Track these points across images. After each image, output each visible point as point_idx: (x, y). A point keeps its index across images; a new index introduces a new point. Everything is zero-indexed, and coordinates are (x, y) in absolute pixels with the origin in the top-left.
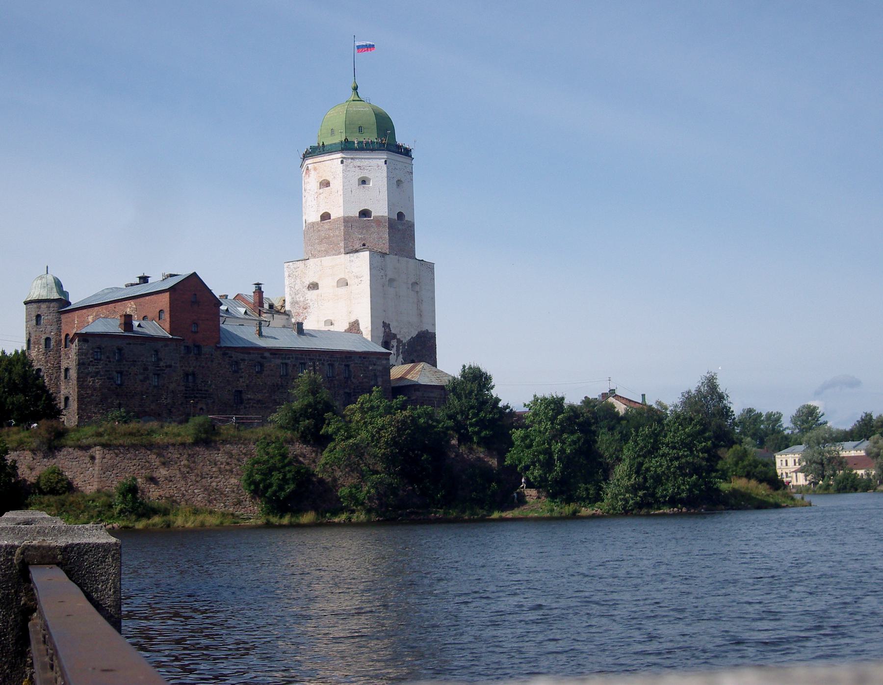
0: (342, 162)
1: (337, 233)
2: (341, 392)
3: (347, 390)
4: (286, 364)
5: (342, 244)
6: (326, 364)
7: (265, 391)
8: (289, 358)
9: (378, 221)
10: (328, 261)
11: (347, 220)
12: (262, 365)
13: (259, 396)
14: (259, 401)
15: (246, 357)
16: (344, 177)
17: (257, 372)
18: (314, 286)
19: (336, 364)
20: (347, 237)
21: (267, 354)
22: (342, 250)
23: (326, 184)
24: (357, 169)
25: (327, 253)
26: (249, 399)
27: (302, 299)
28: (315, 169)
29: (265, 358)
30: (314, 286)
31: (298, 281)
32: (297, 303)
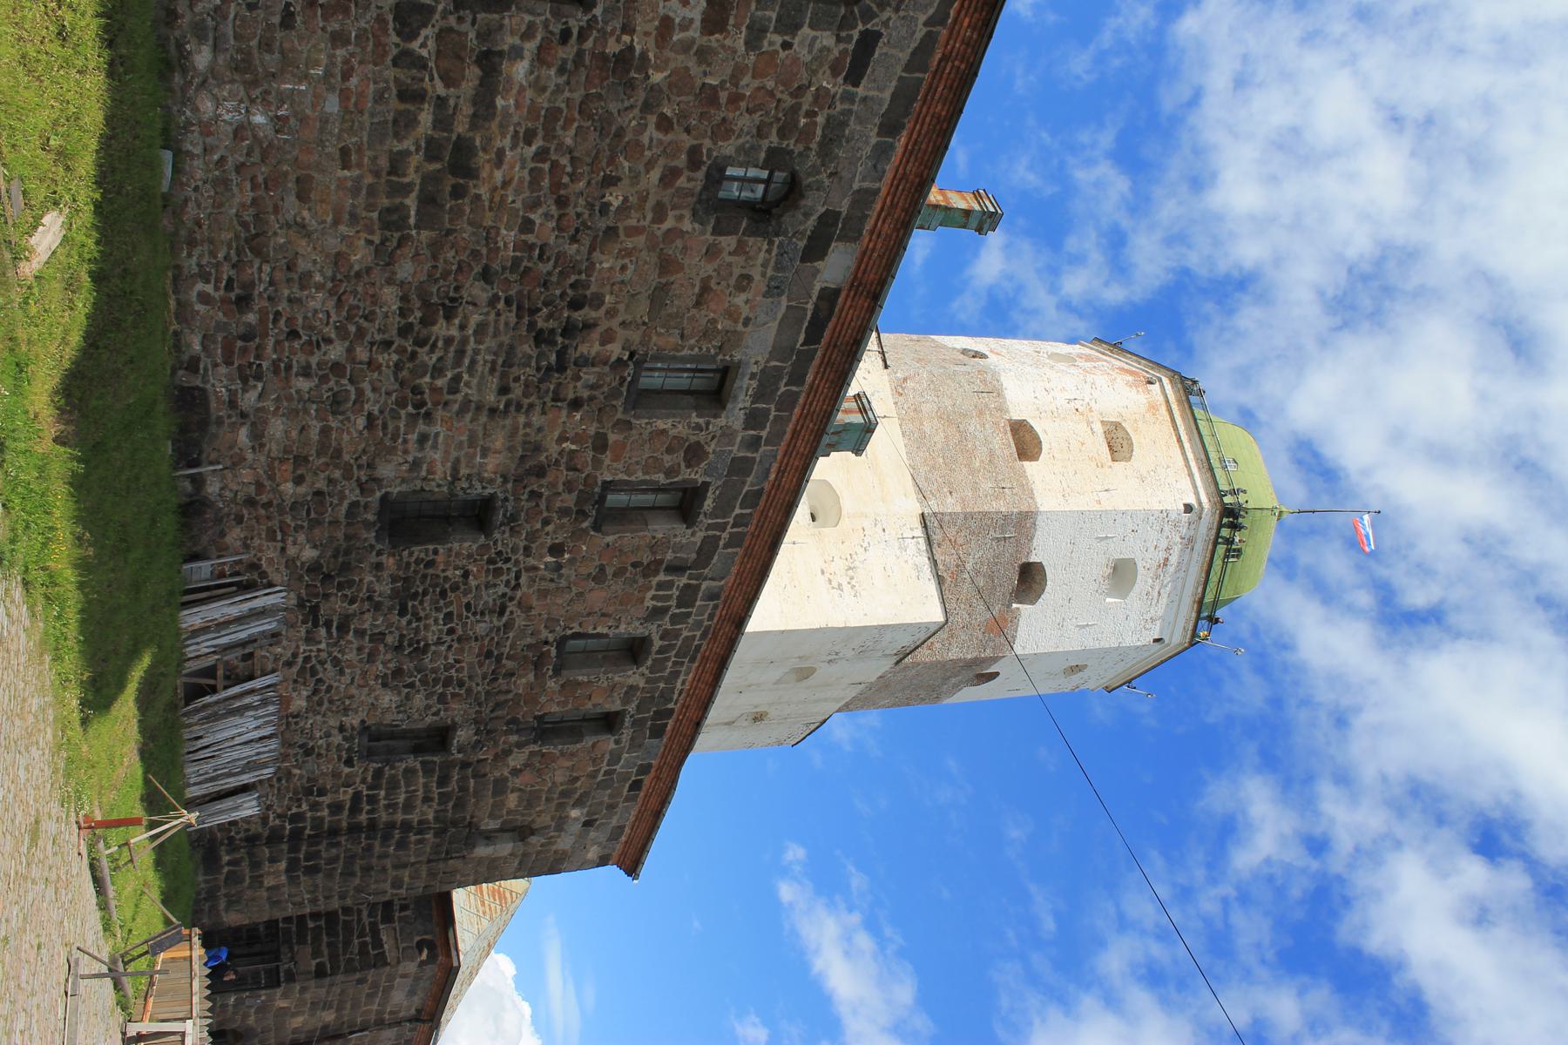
0: (1188, 508)
2: (457, 710)
3: (463, 735)
4: (715, 394)
5: (951, 505)
6: (653, 630)
7: (545, 230)
8: (754, 419)
9: (1001, 628)
11: (1023, 523)
12: (763, 215)
13: (506, 168)
14: (460, 161)
15: (879, 88)
16: (1147, 515)
17: (717, 176)
19: (635, 677)
20: (976, 523)
21: (836, 266)
22: (934, 505)
23: (1118, 443)
24: (1162, 555)
26: (490, 61)
28: (1153, 408)
29: (816, 249)
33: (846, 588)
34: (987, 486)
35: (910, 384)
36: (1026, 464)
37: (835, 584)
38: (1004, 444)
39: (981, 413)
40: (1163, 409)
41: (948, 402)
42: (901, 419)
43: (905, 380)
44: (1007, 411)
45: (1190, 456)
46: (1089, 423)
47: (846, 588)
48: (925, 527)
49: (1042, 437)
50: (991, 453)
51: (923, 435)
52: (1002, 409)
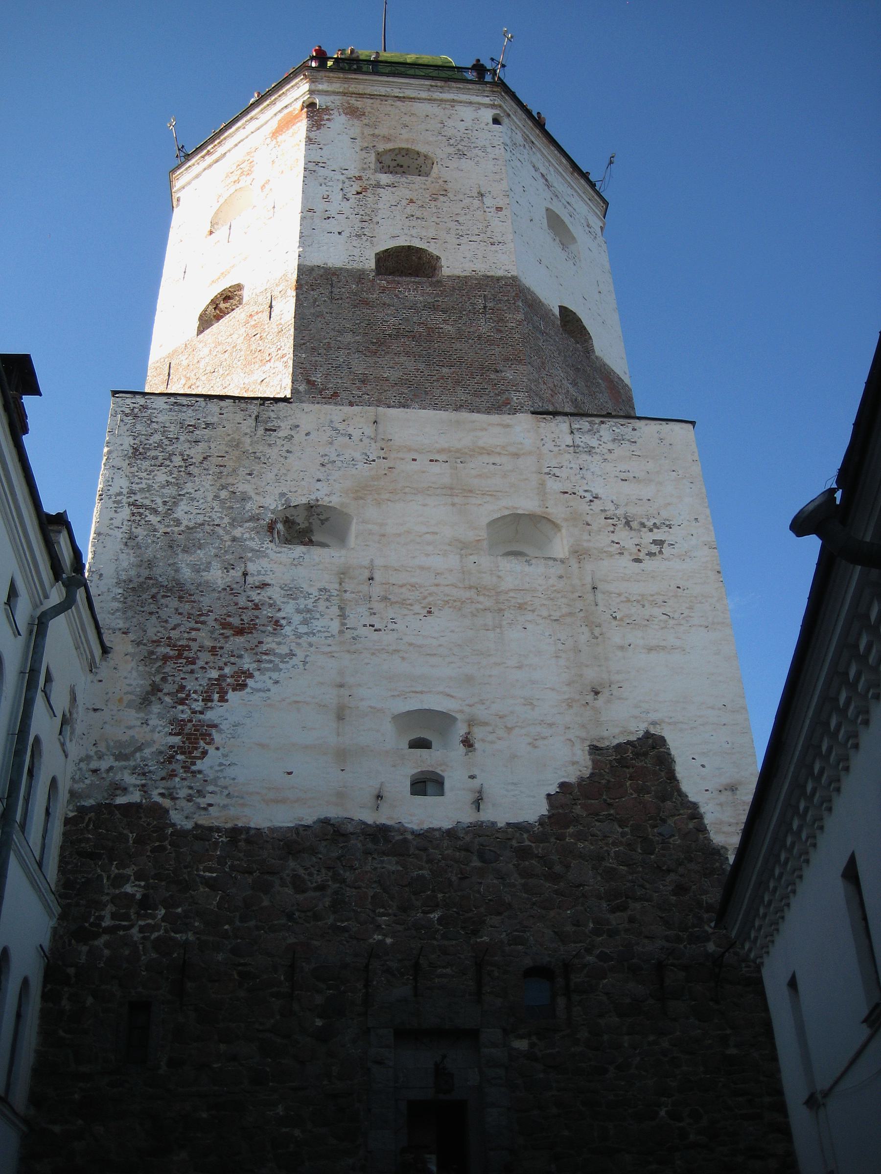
1: (484, 327)
10: (419, 428)
18: (302, 526)
25: (413, 393)
27: (216, 576)
30: (302, 526)
31: (203, 486)
32: (179, 590)
33: (658, 535)
34: (484, 327)
35: (318, 378)
36: (446, 271)
37: (655, 549)
38: (412, 292)
39: (366, 303)
41: (348, 338)
42: (379, 403)
45: (424, 95)
46: (378, 185)
47: (658, 535)
48: (555, 414)
49: (402, 242)
50: (433, 307)
51: (400, 382)
52: (359, 276)
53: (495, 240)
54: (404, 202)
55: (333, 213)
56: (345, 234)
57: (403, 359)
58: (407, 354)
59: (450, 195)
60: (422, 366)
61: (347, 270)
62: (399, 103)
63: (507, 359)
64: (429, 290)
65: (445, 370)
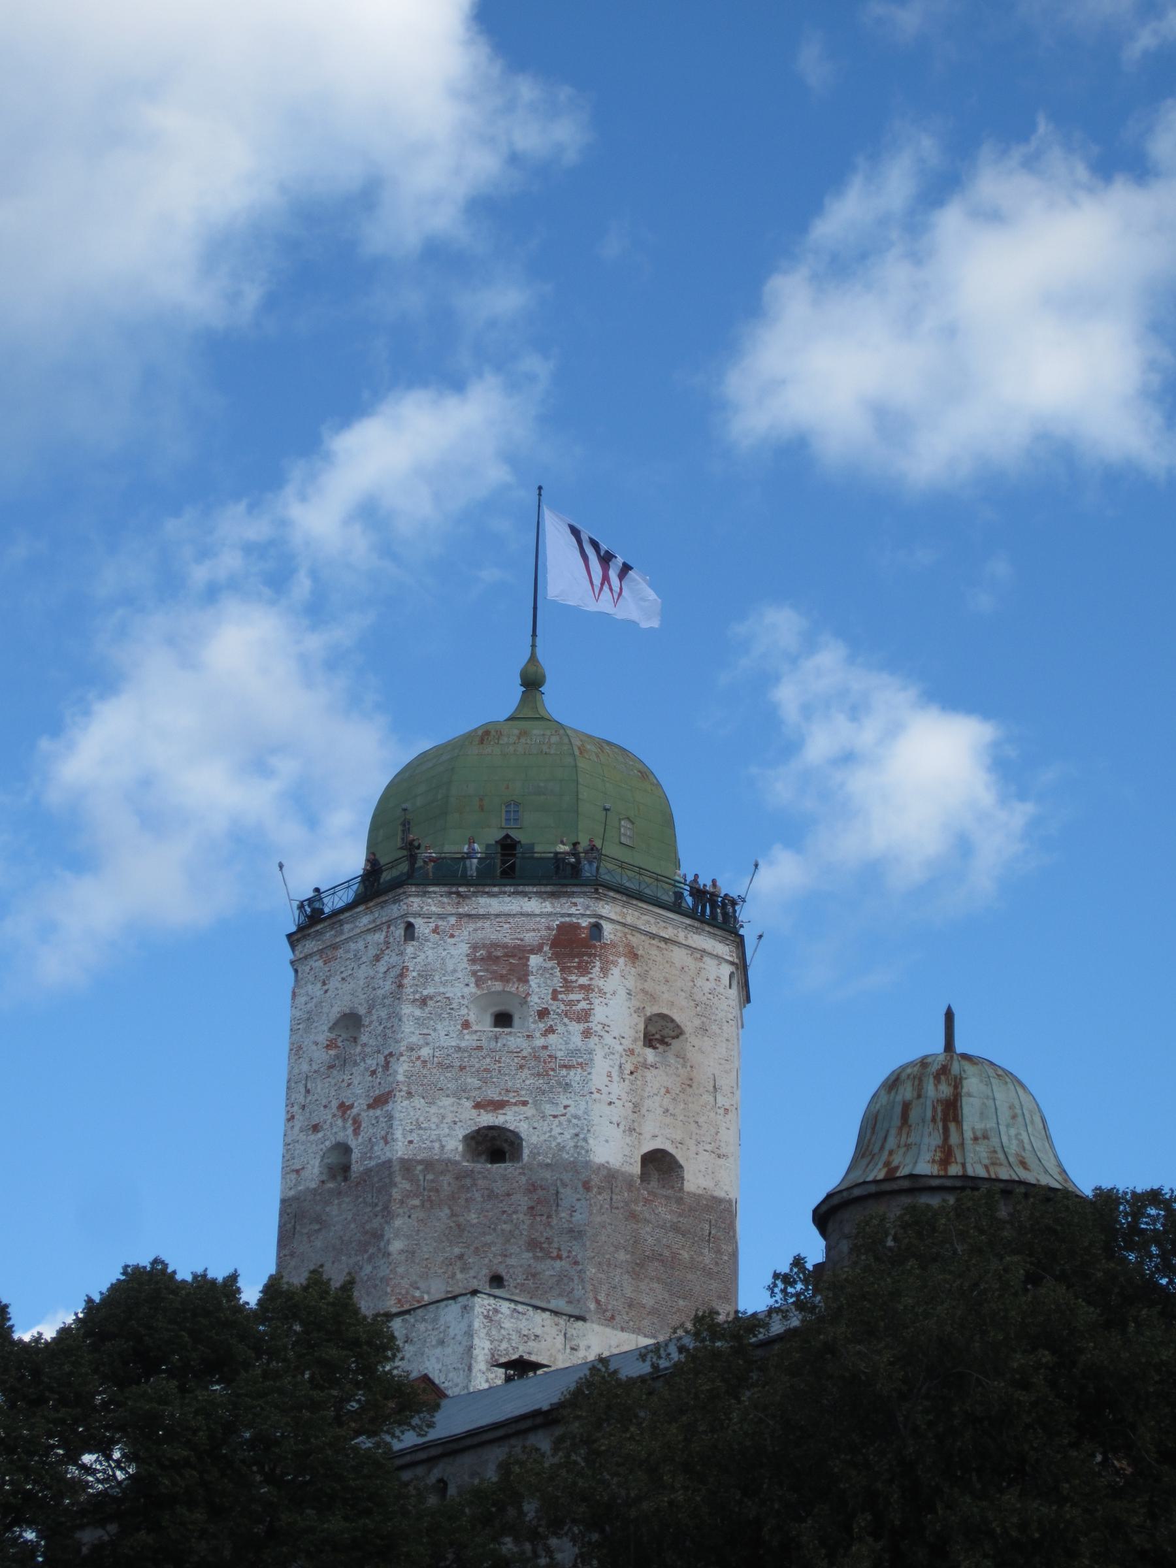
39: (633, 1216)
40: (636, 939)
41: (622, 1256)
43: (598, 1302)
44: (631, 1175)
50: (676, 1228)
53: (723, 1151)
54: (663, 1091)
55: (614, 1098)
56: (622, 1127)
57: (655, 1285)
58: (659, 1280)
59: (695, 1085)
60: (667, 1296)
61: (623, 1174)
62: (662, 945)
63: (719, 1297)
64: (674, 1207)
65: (681, 1302)
